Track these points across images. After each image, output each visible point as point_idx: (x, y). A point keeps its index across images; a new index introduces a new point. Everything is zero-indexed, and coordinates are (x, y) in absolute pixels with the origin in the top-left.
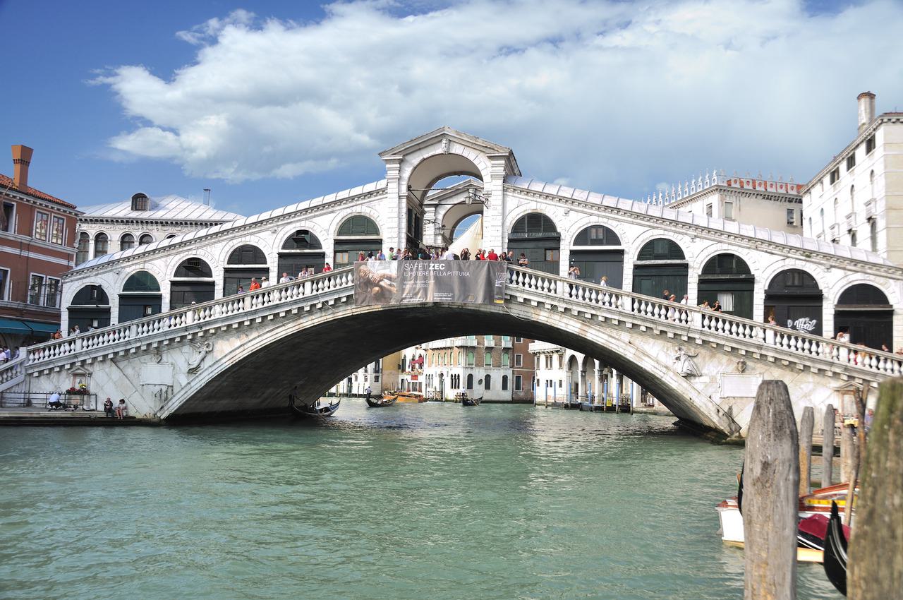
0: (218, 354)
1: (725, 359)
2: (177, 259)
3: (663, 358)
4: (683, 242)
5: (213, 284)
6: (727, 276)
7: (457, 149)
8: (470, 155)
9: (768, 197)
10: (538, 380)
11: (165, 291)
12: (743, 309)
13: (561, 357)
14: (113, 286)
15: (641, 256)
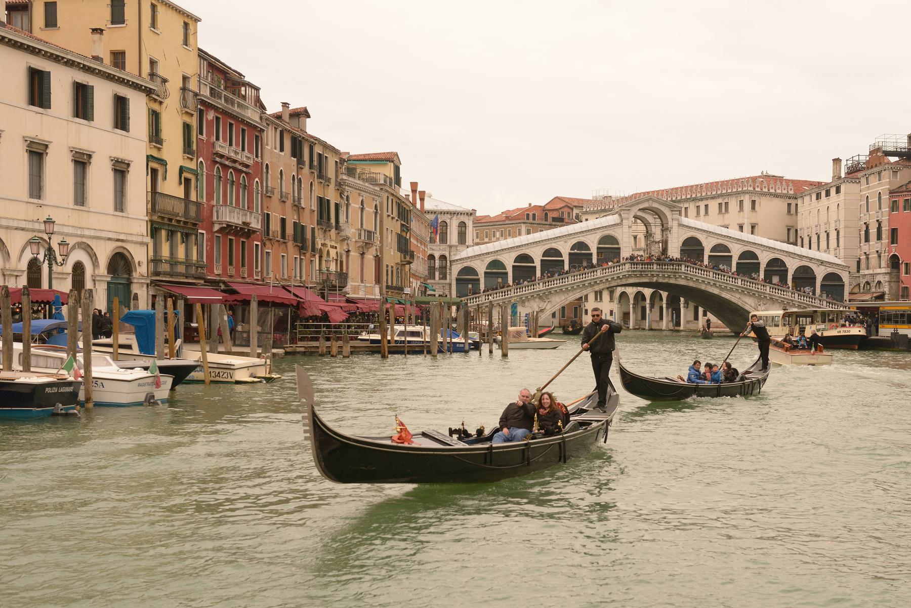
0: (554, 303)
1: (778, 305)
2: (514, 255)
3: (753, 305)
4: (758, 252)
5: (535, 267)
6: (777, 267)
7: (655, 205)
8: (662, 208)
9: (776, 196)
10: (586, 311)
11: (510, 270)
12: (783, 280)
13: (611, 293)
14: (481, 268)
15: (739, 259)
